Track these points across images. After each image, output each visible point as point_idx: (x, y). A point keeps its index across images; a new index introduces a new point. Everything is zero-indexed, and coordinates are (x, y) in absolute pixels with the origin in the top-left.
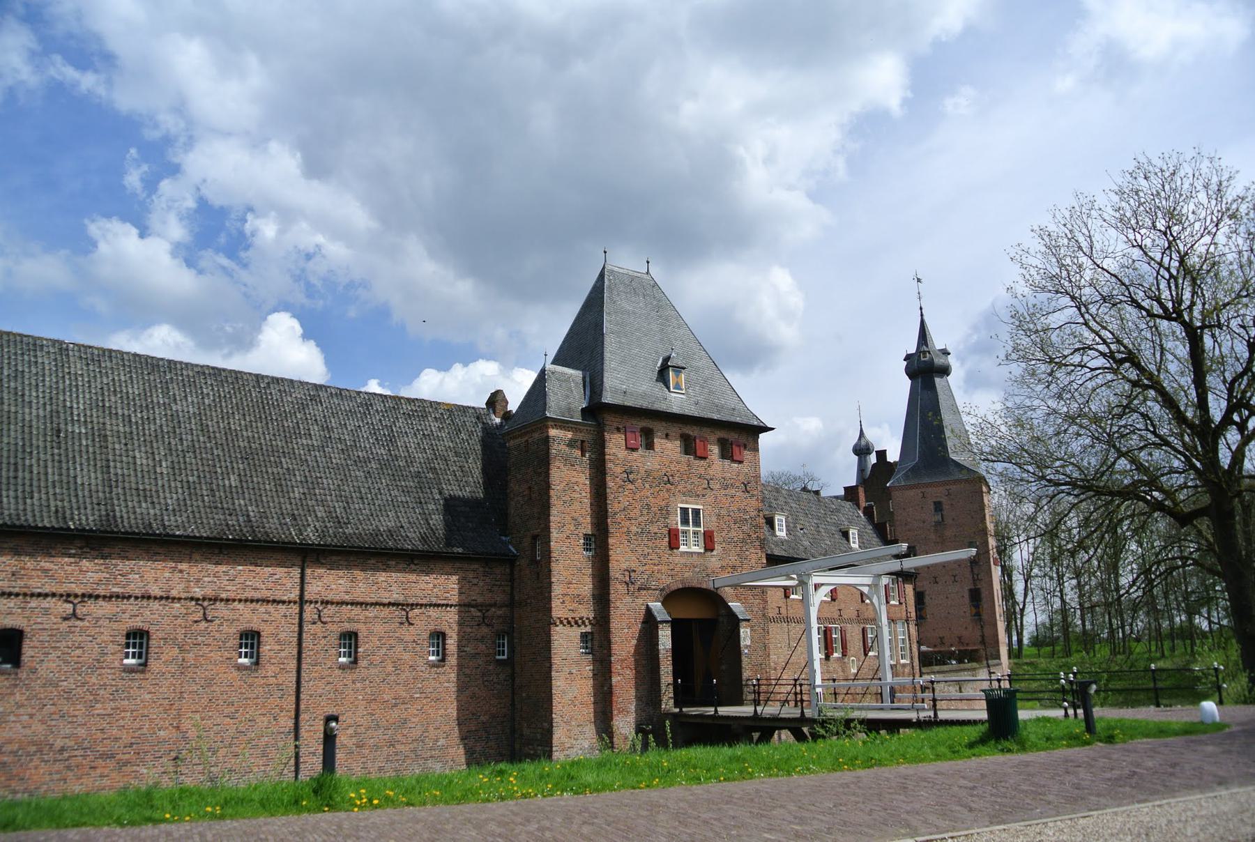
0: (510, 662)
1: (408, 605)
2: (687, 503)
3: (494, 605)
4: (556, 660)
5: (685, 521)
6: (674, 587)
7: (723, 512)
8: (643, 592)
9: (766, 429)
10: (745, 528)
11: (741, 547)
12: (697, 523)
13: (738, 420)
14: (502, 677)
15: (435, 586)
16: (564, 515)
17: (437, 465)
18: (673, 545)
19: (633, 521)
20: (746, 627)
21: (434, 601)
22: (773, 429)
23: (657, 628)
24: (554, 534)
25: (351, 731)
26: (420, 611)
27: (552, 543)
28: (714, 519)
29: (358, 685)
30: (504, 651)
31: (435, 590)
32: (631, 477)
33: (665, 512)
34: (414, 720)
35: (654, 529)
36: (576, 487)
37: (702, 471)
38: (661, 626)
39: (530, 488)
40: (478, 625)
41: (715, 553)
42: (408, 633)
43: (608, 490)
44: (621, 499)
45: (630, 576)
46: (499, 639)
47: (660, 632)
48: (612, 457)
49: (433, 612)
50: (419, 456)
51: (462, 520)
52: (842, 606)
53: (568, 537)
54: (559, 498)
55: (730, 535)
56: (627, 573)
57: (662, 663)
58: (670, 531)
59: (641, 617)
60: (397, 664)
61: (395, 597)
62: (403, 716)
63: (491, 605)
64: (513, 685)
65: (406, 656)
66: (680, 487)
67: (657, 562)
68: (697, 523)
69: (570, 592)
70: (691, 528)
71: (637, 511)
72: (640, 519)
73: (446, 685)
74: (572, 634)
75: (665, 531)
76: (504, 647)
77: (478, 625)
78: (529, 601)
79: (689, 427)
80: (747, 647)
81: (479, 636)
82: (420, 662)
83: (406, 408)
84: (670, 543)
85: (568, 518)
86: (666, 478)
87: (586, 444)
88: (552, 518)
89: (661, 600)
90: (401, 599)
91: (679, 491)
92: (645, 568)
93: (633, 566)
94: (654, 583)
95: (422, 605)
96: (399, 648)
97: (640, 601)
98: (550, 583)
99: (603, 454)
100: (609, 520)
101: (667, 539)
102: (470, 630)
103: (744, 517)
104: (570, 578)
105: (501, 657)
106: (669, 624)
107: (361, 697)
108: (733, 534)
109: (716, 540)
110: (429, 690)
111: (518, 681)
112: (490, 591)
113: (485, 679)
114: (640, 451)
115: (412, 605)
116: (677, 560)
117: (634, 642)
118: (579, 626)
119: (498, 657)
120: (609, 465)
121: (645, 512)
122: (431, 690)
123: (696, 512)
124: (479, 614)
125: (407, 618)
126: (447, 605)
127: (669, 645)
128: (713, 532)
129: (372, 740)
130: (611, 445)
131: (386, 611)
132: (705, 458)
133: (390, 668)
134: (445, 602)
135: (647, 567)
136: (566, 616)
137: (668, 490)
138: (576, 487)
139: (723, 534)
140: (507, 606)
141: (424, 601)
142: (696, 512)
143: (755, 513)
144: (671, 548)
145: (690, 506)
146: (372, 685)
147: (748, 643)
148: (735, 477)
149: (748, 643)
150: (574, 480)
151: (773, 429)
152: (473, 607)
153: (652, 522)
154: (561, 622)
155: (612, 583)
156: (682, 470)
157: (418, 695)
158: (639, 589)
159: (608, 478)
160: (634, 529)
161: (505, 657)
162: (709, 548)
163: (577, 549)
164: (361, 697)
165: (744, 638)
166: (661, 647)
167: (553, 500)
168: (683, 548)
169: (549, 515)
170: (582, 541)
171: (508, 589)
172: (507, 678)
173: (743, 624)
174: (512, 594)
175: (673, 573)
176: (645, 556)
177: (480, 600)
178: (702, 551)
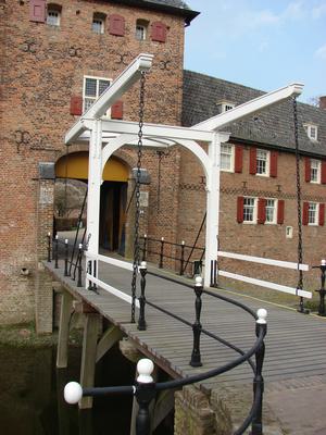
8: (36, 152)
10: (160, 102)
20: (145, 190)
32: (33, 48)
33: (69, 81)
35: (54, 96)
37: (115, 47)
48: (12, 29)
52: (282, 184)
71: (36, 80)
79: (104, 6)
86: (72, 52)
101: (69, 107)
143: (174, 90)
160: (30, 95)
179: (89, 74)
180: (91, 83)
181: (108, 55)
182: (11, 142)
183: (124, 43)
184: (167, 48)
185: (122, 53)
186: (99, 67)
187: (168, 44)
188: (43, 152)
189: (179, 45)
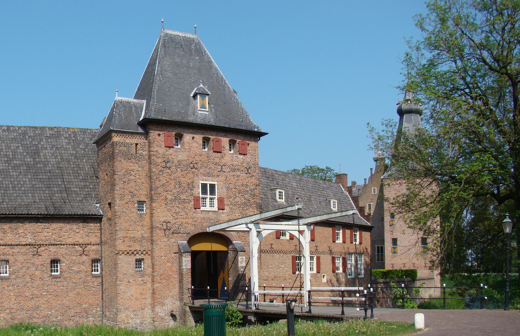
0: (101, 276)
1: (38, 245)
2: (206, 180)
5: (204, 192)
7: (232, 186)
8: (175, 235)
13: (244, 128)
14: (96, 284)
15: (53, 234)
16: (123, 190)
17: (62, 165)
18: (197, 207)
21: (53, 242)
22: (267, 134)
23: (182, 256)
25: (8, 311)
26: (45, 248)
28: (225, 190)
29: (11, 288)
31: (53, 236)
33: (191, 186)
34: (43, 306)
35: (183, 197)
37: (217, 160)
41: (224, 211)
42: (37, 261)
47: (184, 259)
49: (52, 249)
50: (53, 160)
51: (74, 195)
53: (127, 203)
56: (164, 224)
60: (32, 277)
61: (29, 241)
62: (37, 304)
65: (37, 273)
66: (201, 171)
67: (185, 216)
68: (212, 192)
69: (128, 235)
70: (209, 196)
72: (174, 191)
73: (62, 288)
74: (130, 260)
76: (97, 267)
81: (81, 261)
82: (46, 276)
83: (48, 133)
89: (188, 239)
90: (33, 242)
91: (201, 173)
93: (170, 219)
94: (182, 230)
95: (46, 245)
96: (33, 269)
97: (173, 240)
101: (193, 203)
104: (128, 227)
106: (190, 254)
107: (12, 294)
108: (238, 199)
109: (225, 203)
110: (51, 291)
112: (87, 236)
113: (85, 284)
115: (40, 245)
118: (135, 255)
119: (93, 273)
121: (177, 187)
122: (53, 290)
123: (212, 187)
124: (80, 249)
125: (37, 252)
127: (189, 266)
128: (223, 198)
129: (20, 316)
131: (24, 249)
132: (221, 152)
133: (28, 279)
134: (60, 243)
136: (125, 250)
137: (193, 173)
139: (231, 200)
140: (98, 245)
141: (47, 243)
142: (212, 187)
144: (195, 209)
145: (208, 183)
146: (18, 288)
148: (240, 164)
151: (267, 134)
152: (77, 245)
154: (123, 253)
156: (203, 160)
157: (45, 293)
158: (173, 233)
160: (170, 197)
161: (99, 273)
162: (221, 208)
163: (133, 210)
164: (12, 294)
167: (117, 181)
168: (202, 208)
170: (136, 205)
171: (99, 234)
174: (101, 237)
175: (196, 223)
176: (177, 213)
177: (81, 241)
178: (217, 210)
179: (203, 180)
180: (204, 186)
181: (213, 166)
182: (160, 229)
183: (222, 157)
184: (248, 158)
185: (222, 164)
186: (209, 175)
187: (248, 156)
188: (180, 235)
189: (255, 156)
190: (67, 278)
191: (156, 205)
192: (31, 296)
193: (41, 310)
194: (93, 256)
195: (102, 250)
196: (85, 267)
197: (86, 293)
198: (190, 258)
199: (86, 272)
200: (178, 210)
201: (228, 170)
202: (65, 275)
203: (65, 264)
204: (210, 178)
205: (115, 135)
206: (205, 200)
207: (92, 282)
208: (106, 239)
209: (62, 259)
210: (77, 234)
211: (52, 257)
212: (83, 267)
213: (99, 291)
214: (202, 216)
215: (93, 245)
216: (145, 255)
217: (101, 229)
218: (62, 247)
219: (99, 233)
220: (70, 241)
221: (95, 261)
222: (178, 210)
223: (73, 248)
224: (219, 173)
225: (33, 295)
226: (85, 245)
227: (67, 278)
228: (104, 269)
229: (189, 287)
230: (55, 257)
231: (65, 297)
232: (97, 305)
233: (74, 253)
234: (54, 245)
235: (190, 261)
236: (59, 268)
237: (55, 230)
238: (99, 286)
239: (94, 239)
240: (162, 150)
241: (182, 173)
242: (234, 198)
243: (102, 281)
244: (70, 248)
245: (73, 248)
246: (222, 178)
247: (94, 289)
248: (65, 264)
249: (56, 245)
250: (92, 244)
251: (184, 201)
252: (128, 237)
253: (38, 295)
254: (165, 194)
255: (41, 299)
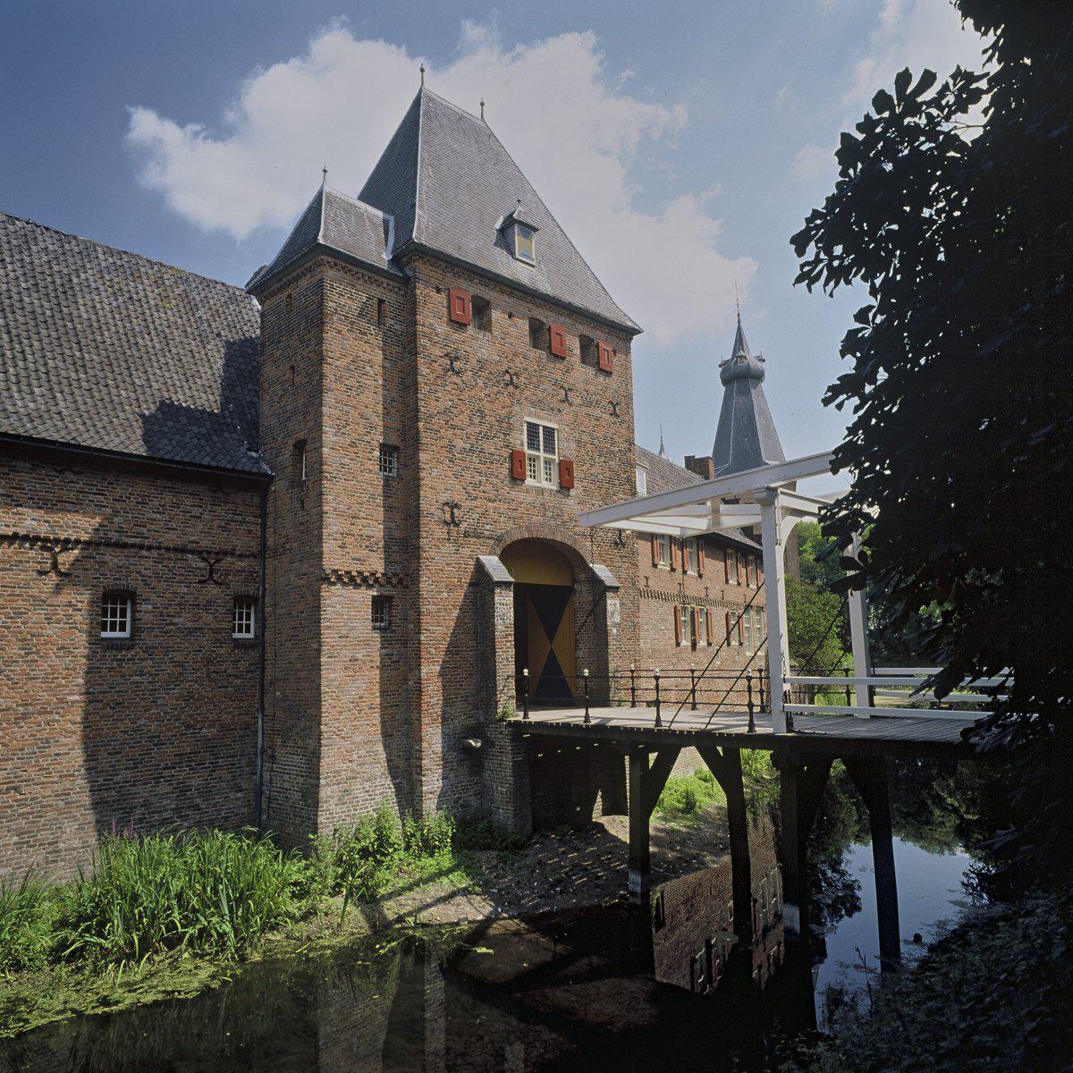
0: (258, 644)
3: (232, 554)
4: (328, 637)
5: (533, 443)
6: (517, 536)
9: (639, 332)
11: (607, 489)
12: (550, 448)
14: (243, 665)
16: (346, 408)
18: (516, 477)
19: (459, 432)
24: (329, 436)
27: (325, 450)
28: (573, 445)
30: (248, 627)
31: (115, 519)
32: (457, 365)
33: (506, 425)
35: (489, 447)
36: (368, 368)
38: (497, 591)
39: (292, 368)
40: (200, 582)
41: (572, 492)
43: (420, 379)
44: (439, 394)
45: (452, 513)
46: (241, 608)
47: (497, 599)
54: (339, 379)
55: (593, 471)
56: (447, 508)
57: (498, 645)
58: (512, 456)
59: (466, 579)
63: (225, 553)
64: (263, 680)
65: (50, 630)
66: (527, 393)
68: (550, 448)
70: (542, 454)
75: (506, 453)
76: (248, 619)
77: (200, 582)
78: (288, 546)
80: (615, 625)
81: (202, 602)
84: (511, 470)
85: (354, 414)
86: (507, 377)
87: (387, 307)
88: (325, 410)
91: (526, 399)
92: (474, 503)
93: (458, 498)
94: (488, 527)
97: (466, 551)
98: (321, 514)
99: (415, 323)
100: (421, 424)
102: (185, 590)
103: (612, 449)
105: (244, 635)
110: (100, 689)
111: (269, 672)
112: (224, 529)
114: (471, 330)
116: (521, 496)
117: (456, 613)
119: (236, 635)
120: (423, 341)
121: (477, 421)
123: (549, 432)
124: (203, 565)
126: (141, 547)
127: (510, 616)
130: (426, 312)
134: (138, 540)
135: (478, 503)
136: (346, 569)
137: (510, 395)
138: (368, 368)
140: (255, 557)
147: (617, 619)
149: (617, 619)
150: (365, 357)
152: (192, 552)
153: (486, 437)
154: (339, 578)
155: (423, 520)
159: (421, 361)
160: (460, 444)
161: (251, 635)
162: (565, 486)
163: (369, 465)
165: (613, 613)
166: (498, 621)
167: (329, 382)
168: (529, 481)
169: (321, 405)
170: (377, 454)
172: (253, 668)
173: (609, 594)
174: (263, 538)
177: (205, 543)
179: (530, 415)
180: (532, 429)
184: (613, 383)
190: (156, 648)
191: (428, 457)
192: (21, 709)
193: (56, 755)
194: (237, 586)
195: (267, 571)
196: (215, 618)
197: (214, 695)
198: (512, 599)
199: (219, 631)
200: (477, 478)
201: (579, 401)
202: (148, 639)
203: (150, 607)
204: (542, 413)
205: (328, 262)
206: (532, 463)
207: (231, 661)
208: (284, 540)
209: (141, 590)
210: (192, 521)
211: (109, 582)
212: (207, 618)
213: (253, 686)
214: (529, 499)
215: (240, 556)
216: (395, 586)
217: (264, 515)
218: (144, 553)
219: (258, 524)
220: (171, 538)
221: (242, 601)
222: (477, 478)
223: (179, 559)
224: (562, 406)
225: (31, 705)
226: (217, 553)
227: (156, 648)
228: (269, 623)
229: (510, 673)
230: (118, 582)
231: (144, 706)
232: (245, 729)
233: (183, 575)
234: (117, 545)
235: (512, 606)
236: (128, 619)
237: (125, 501)
238: (253, 671)
239: (242, 540)
240: (442, 328)
241: (486, 392)
242: (592, 466)
243: (263, 659)
244: (170, 559)
245: (179, 559)
246: (570, 418)
247: (239, 681)
248: (150, 607)
249: (125, 546)
250: (238, 553)
251: (487, 459)
252: (353, 535)
253: (49, 704)
254: (450, 432)
255: (57, 717)
